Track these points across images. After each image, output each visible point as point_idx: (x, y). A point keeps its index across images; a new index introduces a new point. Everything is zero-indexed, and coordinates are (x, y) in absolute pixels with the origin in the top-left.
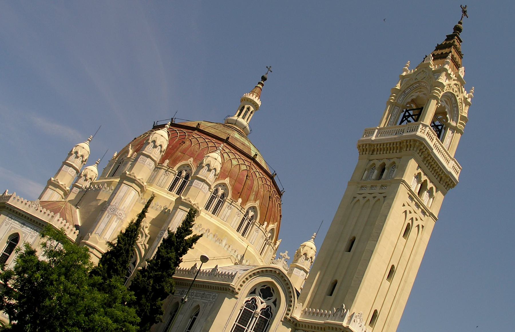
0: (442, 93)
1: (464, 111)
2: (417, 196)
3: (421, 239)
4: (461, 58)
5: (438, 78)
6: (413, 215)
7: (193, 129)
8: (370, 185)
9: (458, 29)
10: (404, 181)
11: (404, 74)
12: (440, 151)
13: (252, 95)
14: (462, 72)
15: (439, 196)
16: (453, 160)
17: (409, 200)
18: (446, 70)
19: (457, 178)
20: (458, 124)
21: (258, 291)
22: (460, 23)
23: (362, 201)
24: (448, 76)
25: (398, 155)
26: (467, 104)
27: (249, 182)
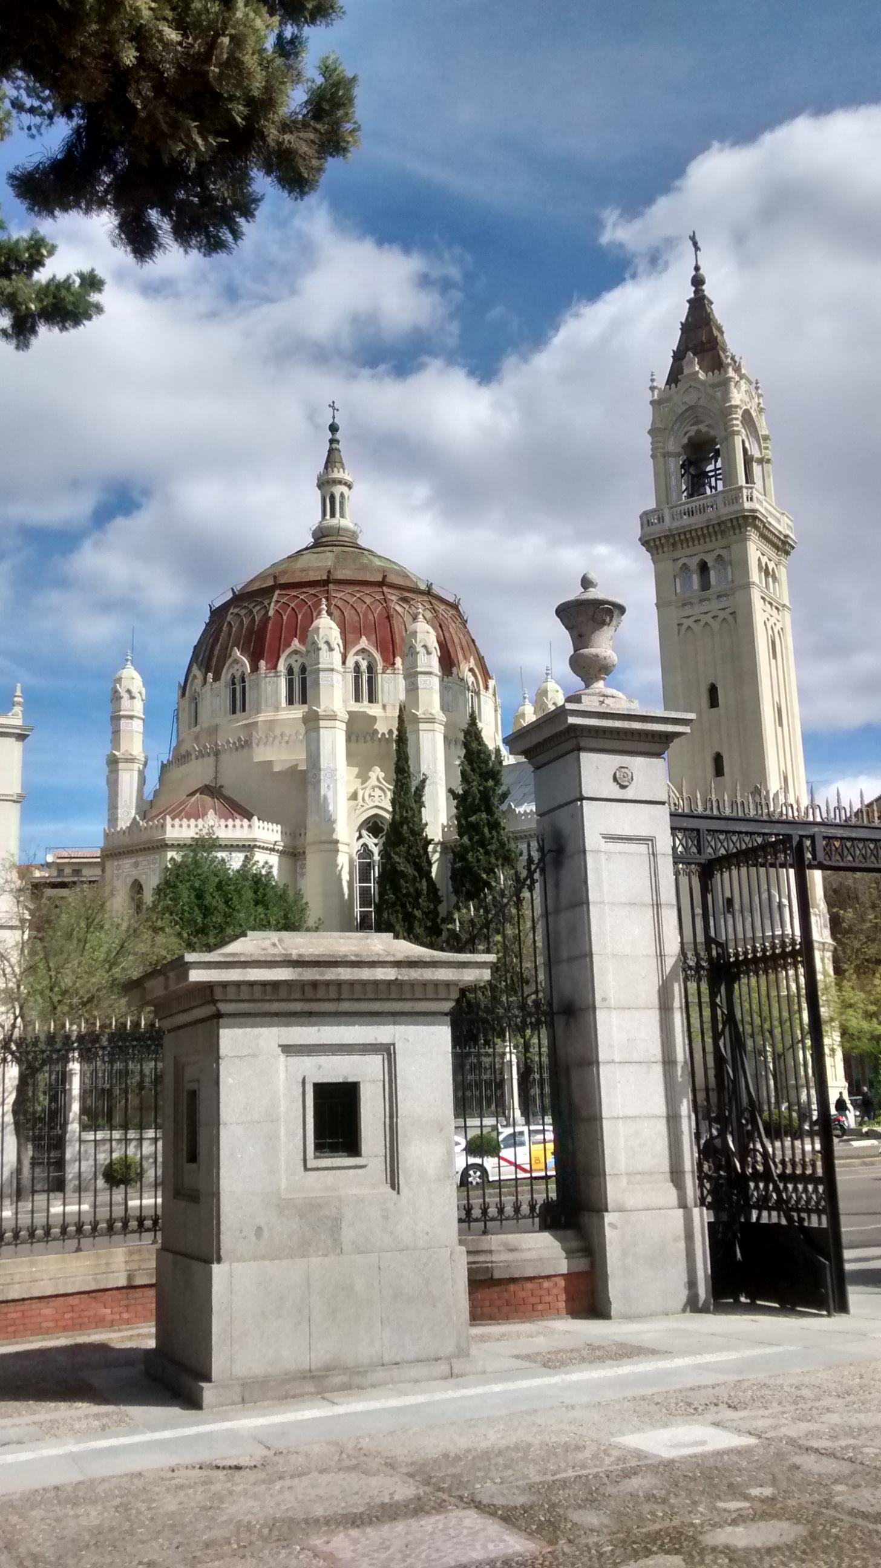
6: (772, 620)
7: (326, 582)
13: (336, 470)
25: (721, 542)
27: (447, 635)
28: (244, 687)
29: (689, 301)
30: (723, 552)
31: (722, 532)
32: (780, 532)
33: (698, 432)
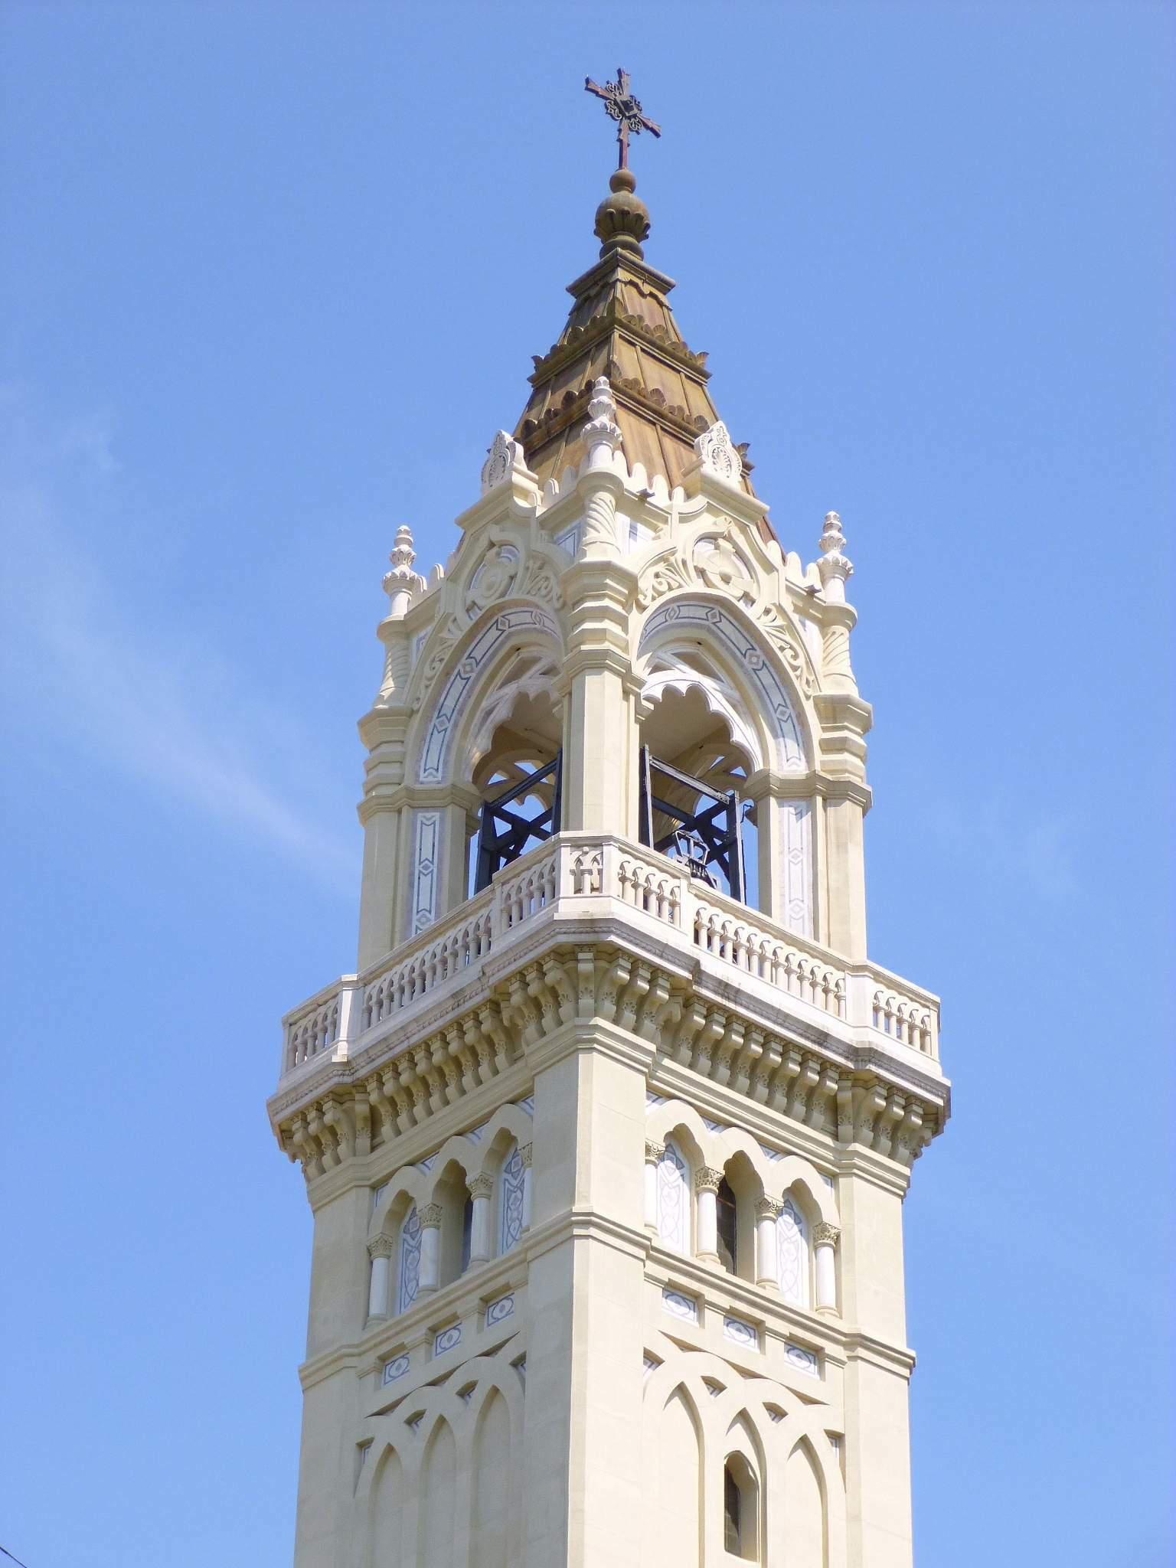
0: (637, 621)
1: (826, 665)
2: (721, 1271)
3: (854, 1518)
4: (698, 375)
5: (579, 549)
8: (421, 1332)
9: (619, 226)
10: (589, 1220)
11: (401, 606)
12: (762, 961)
14: (718, 456)
15: (870, 1211)
16: (858, 969)
17: (679, 1317)
18: (607, 481)
19: (929, 1065)
20: (818, 755)
22: (620, 183)
23: (411, 1446)
24: (638, 506)
25: (510, 1080)
26: (827, 618)
29: (573, 290)
30: (506, 1118)
31: (512, 1034)
32: (822, 1038)
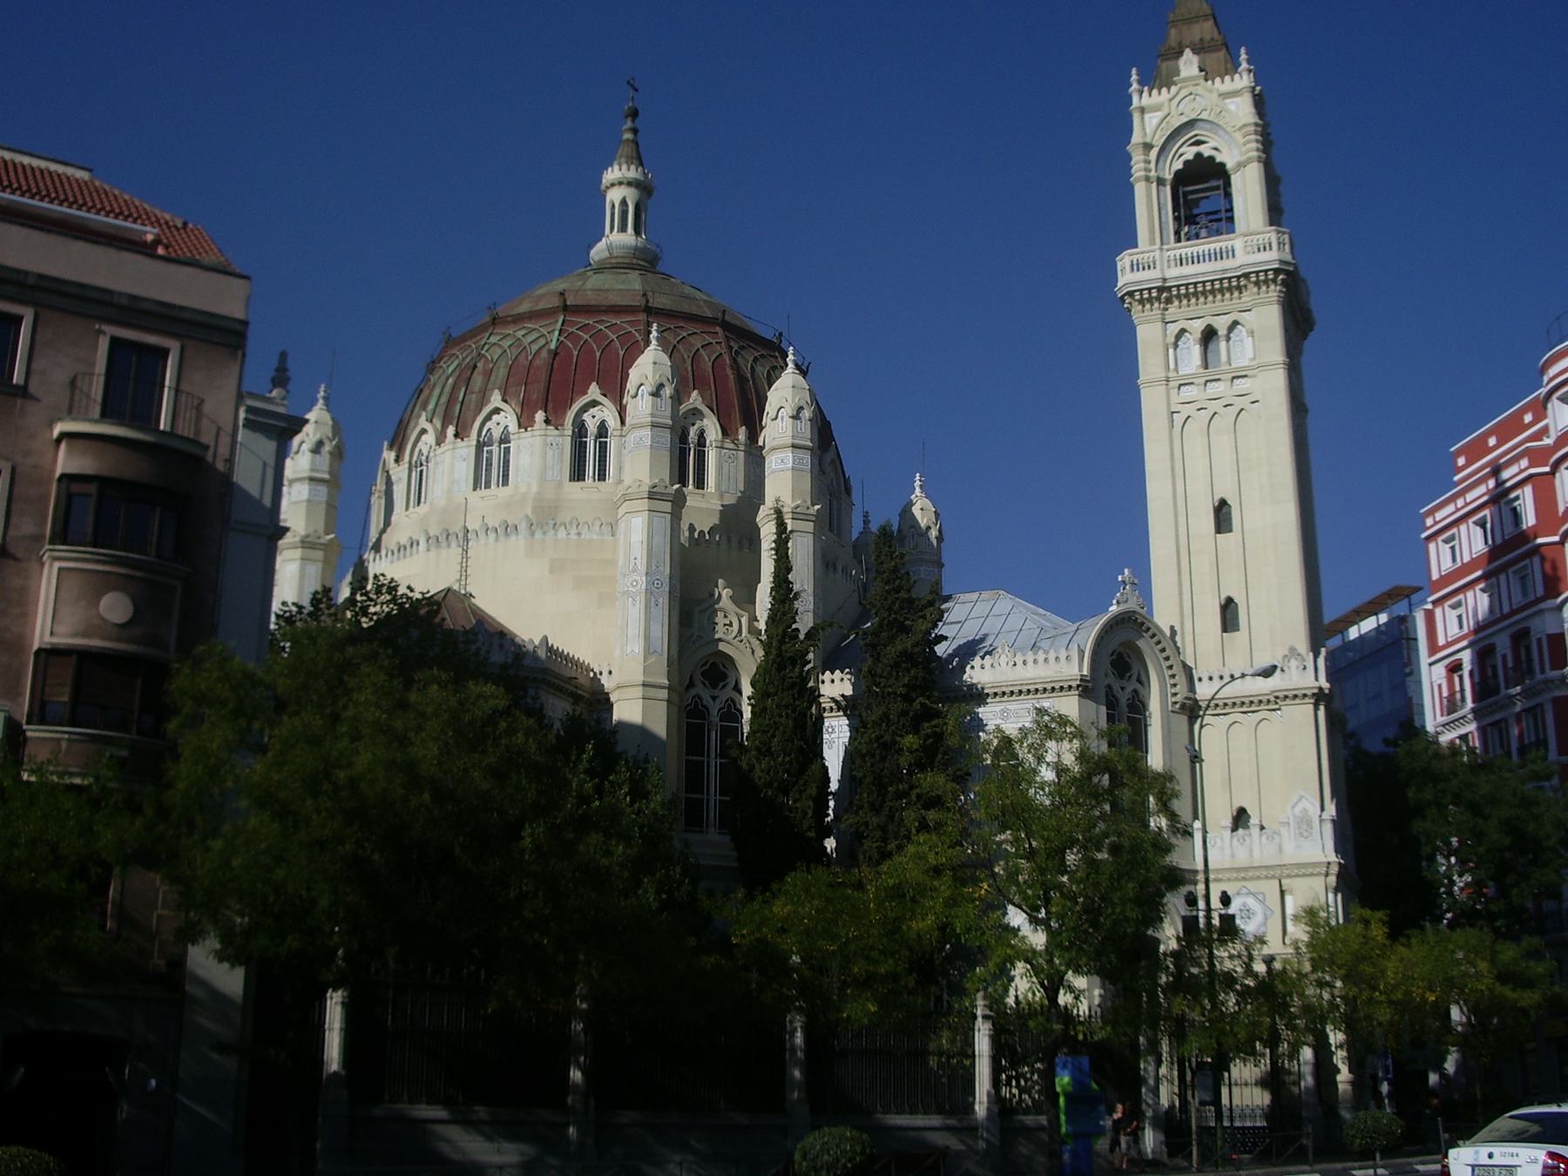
21: (1110, 670)
28: (507, 450)
31: (1239, 288)
33: (1199, 155)
